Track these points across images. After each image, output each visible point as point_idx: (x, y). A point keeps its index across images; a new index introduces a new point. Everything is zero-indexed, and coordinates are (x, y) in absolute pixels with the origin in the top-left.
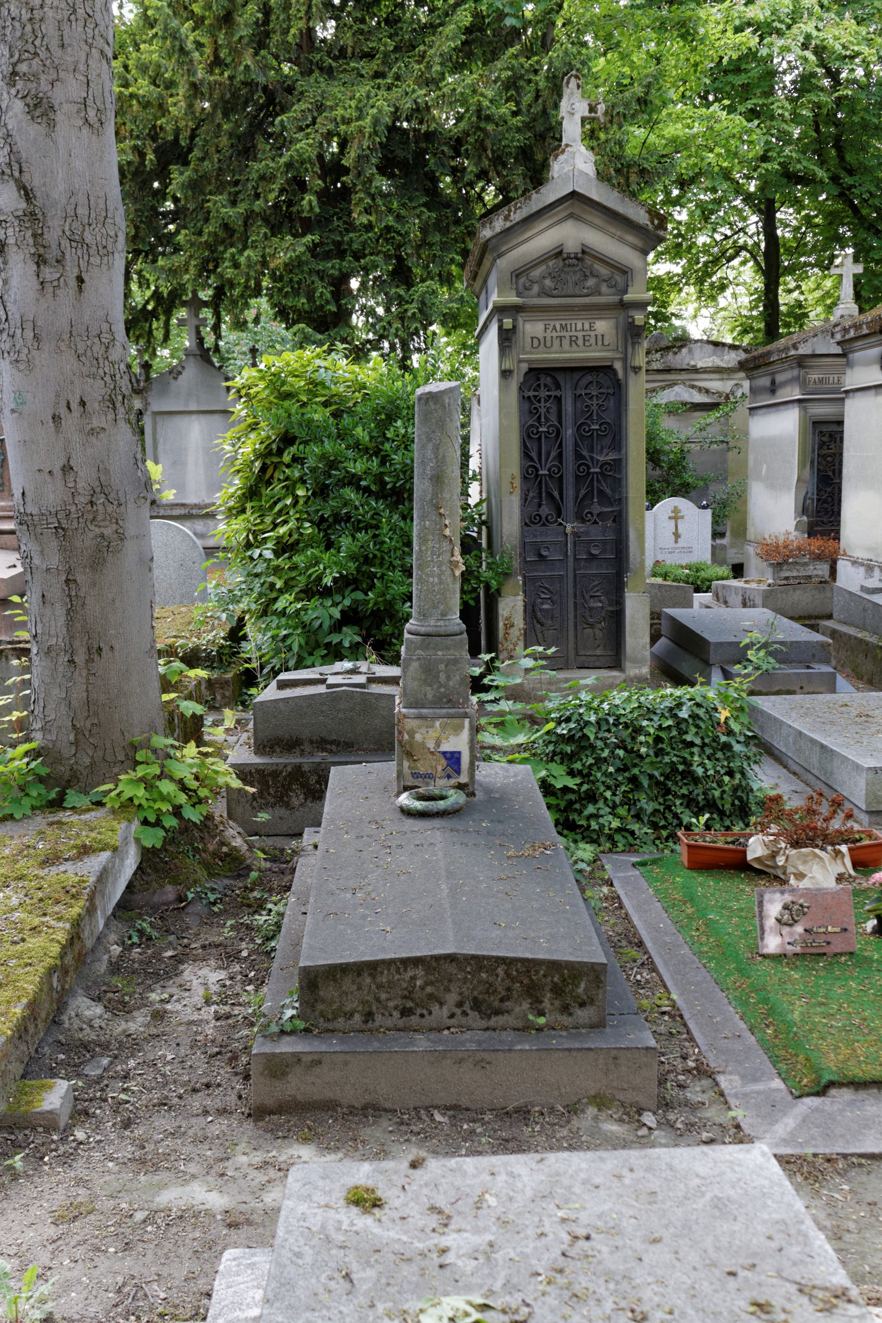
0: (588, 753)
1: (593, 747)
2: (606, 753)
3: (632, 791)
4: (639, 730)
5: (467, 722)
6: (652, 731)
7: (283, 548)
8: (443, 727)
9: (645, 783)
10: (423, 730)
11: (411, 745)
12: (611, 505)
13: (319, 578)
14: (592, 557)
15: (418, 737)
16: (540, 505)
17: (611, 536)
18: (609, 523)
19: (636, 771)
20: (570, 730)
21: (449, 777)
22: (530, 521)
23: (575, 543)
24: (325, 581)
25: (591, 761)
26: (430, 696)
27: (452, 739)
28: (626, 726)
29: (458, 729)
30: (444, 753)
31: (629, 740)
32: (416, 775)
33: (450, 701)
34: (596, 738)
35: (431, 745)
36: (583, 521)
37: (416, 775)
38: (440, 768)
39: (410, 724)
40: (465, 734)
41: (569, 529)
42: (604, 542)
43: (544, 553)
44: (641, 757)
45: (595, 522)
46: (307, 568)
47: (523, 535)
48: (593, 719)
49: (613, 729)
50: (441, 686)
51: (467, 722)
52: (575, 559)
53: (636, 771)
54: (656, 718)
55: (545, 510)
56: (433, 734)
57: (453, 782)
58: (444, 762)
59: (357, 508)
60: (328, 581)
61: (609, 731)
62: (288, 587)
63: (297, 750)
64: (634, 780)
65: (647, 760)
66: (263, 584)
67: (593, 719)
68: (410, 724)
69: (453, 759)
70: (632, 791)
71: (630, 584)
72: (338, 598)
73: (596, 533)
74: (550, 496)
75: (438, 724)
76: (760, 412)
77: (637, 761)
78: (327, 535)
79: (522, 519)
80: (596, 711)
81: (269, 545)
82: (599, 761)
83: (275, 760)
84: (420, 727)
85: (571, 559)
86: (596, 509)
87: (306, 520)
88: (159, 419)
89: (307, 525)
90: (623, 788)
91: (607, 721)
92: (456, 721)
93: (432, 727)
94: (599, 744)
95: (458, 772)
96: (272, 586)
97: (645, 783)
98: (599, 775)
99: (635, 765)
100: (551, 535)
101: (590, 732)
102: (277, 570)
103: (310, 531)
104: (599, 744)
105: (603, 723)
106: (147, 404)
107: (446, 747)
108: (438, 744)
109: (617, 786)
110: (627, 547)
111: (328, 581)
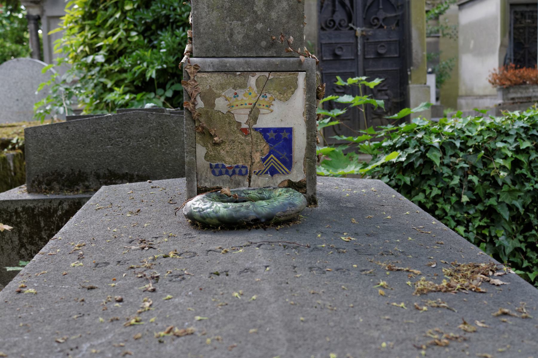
0: (432, 182)
1: (437, 175)
2: (456, 180)
3: (488, 227)
4: (491, 154)
5: (301, 77)
6: (510, 154)
7: (113, 55)
8: (262, 88)
9: (506, 214)
10: (229, 92)
11: (210, 119)
12: (395, 11)
13: (143, 74)
14: (379, 56)
15: (220, 104)
16: (334, 12)
17: (394, 37)
18: (393, 27)
19: (492, 201)
20: (409, 156)
21: (273, 172)
22: (327, 25)
23: (364, 46)
24: (148, 76)
25: (436, 191)
26: (239, 38)
27: (277, 106)
28: (477, 150)
30: (264, 131)
31: (480, 166)
32: (217, 170)
33: (273, 44)
34: (442, 164)
36: (371, 25)
37: (217, 170)
38: (257, 157)
39: (208, 81)
40: (299, 99)
42: (389, 43)
43: (338, 52)
44: (495, 184)
45: (381, 27)
46: (133, 66)
47: (320, 38)
48: (436, 142)
49: (461, 154)
50: (257, 18)
51: (301, 77)
52: (365, 59)
53: (492, 201)
54: (511, 140)
55: (340, 16)
56: (246, 98)
57: (279, 179)
58: (264, 147)
59: (175, 10)
60: (152, 73)
61: (455, 155)
62: (117, 84)
63: (81, 187)
64: (490, 213)
65: (505, 188)
66: (96, 85)
67: (436, 142)
68: (208, 81)
70: (488, 227)
71: (413, 77)
72: (160, 91)
73: (381, 35)
74: (343, 5)
75: (252, 81)
76: (467, 5)
77: (491, 191)
78: (150, 41)
79: (319, 23)
80: (438, 135)
81: (102, 52)
82: (447, 190)
84: (223, 87)
85: (361, 58)
86: (382, 15)
87: (132, 30)
88: (52, 21)
89: (134, 34)
90: (477, 223)
91: (454, 146)
92: (283, 76)
93: (243, 86)
94: (446, 171)
95: (288, 163)
96: (104, 86)
97: (506, 214)
98: (448, 208)
99: (489, 196)
100: (344, 37)
101: (435, 157)
102: (108, 74)
103: (136, 39)
104: (446, 171)
105: (448, 148)
106: (43, 11)
107: (266, 121)
108: (254, 116)
109: (469, 221)
110: (410, 45)
111: (152, 73)
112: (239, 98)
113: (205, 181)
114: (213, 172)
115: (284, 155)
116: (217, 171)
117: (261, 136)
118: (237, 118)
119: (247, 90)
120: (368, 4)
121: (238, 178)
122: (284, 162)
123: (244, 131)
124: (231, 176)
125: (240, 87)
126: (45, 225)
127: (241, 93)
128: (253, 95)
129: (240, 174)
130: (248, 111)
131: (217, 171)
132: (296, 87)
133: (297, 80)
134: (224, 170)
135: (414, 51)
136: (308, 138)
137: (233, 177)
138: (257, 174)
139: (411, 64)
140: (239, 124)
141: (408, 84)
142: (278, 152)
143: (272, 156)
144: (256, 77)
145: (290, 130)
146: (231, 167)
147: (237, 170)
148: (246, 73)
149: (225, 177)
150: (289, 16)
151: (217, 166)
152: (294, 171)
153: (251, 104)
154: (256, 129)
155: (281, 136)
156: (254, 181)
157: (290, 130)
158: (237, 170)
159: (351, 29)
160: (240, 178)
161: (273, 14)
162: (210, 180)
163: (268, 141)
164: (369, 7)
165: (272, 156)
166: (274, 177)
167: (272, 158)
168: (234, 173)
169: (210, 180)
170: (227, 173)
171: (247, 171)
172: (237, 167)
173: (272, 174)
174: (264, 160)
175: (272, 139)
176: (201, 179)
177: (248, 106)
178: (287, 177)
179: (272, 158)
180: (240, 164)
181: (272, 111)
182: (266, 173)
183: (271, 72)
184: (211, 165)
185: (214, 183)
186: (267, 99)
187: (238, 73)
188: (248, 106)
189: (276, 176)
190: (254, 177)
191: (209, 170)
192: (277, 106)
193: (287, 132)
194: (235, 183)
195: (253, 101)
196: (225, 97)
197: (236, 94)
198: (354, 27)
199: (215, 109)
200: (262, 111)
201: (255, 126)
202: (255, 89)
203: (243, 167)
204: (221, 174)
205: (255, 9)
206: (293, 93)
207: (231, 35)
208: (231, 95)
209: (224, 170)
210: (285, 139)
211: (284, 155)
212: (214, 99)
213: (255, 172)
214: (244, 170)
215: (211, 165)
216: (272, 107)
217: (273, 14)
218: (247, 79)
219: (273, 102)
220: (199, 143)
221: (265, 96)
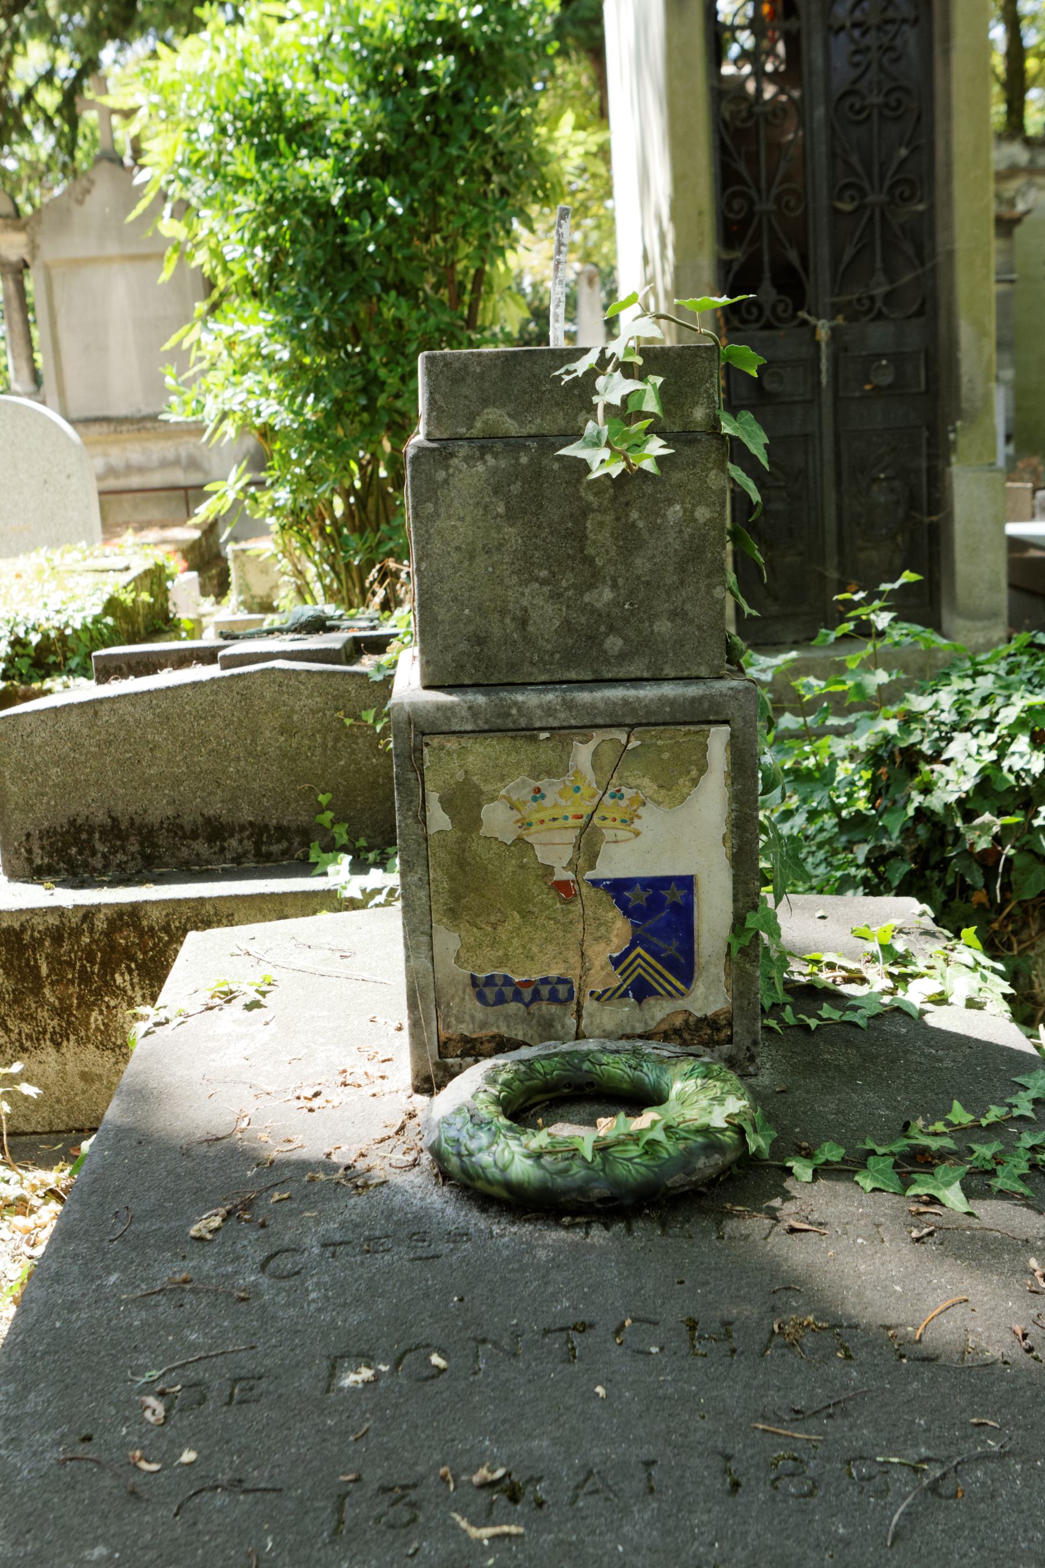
5: (718, 738)
8: (612, 767)
10: (519, 786)
15: (497, 820)
21: (642, 991)
29: (680, 774)
30: (618, 888)
35: (556, 852)
38: (601, 953)
40: (711, 798)
41: (823, 333)
56: (565, 803)
57: (659, 1011)
58: (619, 930)
69: (660, 910)
75: (583, 754)
83: (67, 898)
85: (827, 398)
92: (665, 739)
95: (684, 968)
106: (34, 247)
107: (623, 860)
108: (588, 843)
112: (547, 802)
113: (460, 1020)
114: (481, 997)
115: (671, 948)
116: (490, 993)
117: (607, 898)
118: (543, 855)
119: (568, 779)
120: (846, 258)
121: (547, 1009)
122: (671, 965)
123: (562, 886)
124: (527, 1005)
125: (549, 774)
126: (52, 970)
127: (552, 788)
128: (585, 791)
129: (554, 998)
130: (571, 836)
131: (490, 993)
132: (703, 769)
133: (705, 748)
134: (508, 991)
135: (964, 380)
136: (735, 900)
137: (534, 1008)
138: (598, 999)
139: (958, 413)
140: (549, 870)
141: (948, 464)
142: (655, 940)
143: (639, 950)
144: (592, 745)
145: (687, 883)
146: (527, 983)
147: (545, 991)
148: (564, 733)
149: (513, 1007)
150: (681, 568)
151: (490, 980)
152: (700, 988)
153: (580, 817)
154: (595, 883)
155: (664, 898)
156: (591, 1016)
157: (687, 883)
158: (545, 991)
159: (804, 323)
160: (554, 1008)
161: (638, 561)
162: (472, 1017)
163: (627, 913)
164: (849, 265)
165: (639, 950)
166: (644, 1005)
167: (639, 956)
168: (536, 996)
169: (472, 1017)
170: (517, 996)
171: (571, 992)
172: (545, 981)
173: (639, 999)
174: (616, 962)
175: (639, 906)
176: (447, 1016)
177: (571, 822)
178: (681, 1004)
179: (639, 956)
180: (554, 973)
181: (637, 834)
182: (625, 995)
183: (632, 726)
184: (473, 977)
185: (483, 1025)
186: (623, 803)
187: (544, 735)
188: (571, 822)
189: (652, 1001)
190: (589, 1004)
191: (469, 990)
192: (649, 819)
193: (679, 887)
194: (539, 1024)
195: (585, 809)
196: (508, 798)
197: (538, 790)
198: (812, 320)
199: (483, 832)
200: (609, 834)
201: (590, 875)
202: (590, 775)
203: (561, 981)
204: (501, 1000)
205: (590, 551)
206: (695, 782)
207: (523, 622)
208: (526, 794)
209: (508, 991)
210: (675, 904)
211: (671, 948)
212: (480, 806)
213: (592, 993)
214: (562, 989)
215: (473, 977)
216: (637, 824)
217: (638, 561)
218: (565, 749)
219: (642, 811)
220: (439, 921)
221: (618, 795)
